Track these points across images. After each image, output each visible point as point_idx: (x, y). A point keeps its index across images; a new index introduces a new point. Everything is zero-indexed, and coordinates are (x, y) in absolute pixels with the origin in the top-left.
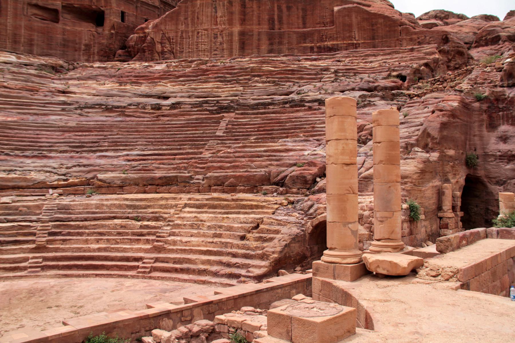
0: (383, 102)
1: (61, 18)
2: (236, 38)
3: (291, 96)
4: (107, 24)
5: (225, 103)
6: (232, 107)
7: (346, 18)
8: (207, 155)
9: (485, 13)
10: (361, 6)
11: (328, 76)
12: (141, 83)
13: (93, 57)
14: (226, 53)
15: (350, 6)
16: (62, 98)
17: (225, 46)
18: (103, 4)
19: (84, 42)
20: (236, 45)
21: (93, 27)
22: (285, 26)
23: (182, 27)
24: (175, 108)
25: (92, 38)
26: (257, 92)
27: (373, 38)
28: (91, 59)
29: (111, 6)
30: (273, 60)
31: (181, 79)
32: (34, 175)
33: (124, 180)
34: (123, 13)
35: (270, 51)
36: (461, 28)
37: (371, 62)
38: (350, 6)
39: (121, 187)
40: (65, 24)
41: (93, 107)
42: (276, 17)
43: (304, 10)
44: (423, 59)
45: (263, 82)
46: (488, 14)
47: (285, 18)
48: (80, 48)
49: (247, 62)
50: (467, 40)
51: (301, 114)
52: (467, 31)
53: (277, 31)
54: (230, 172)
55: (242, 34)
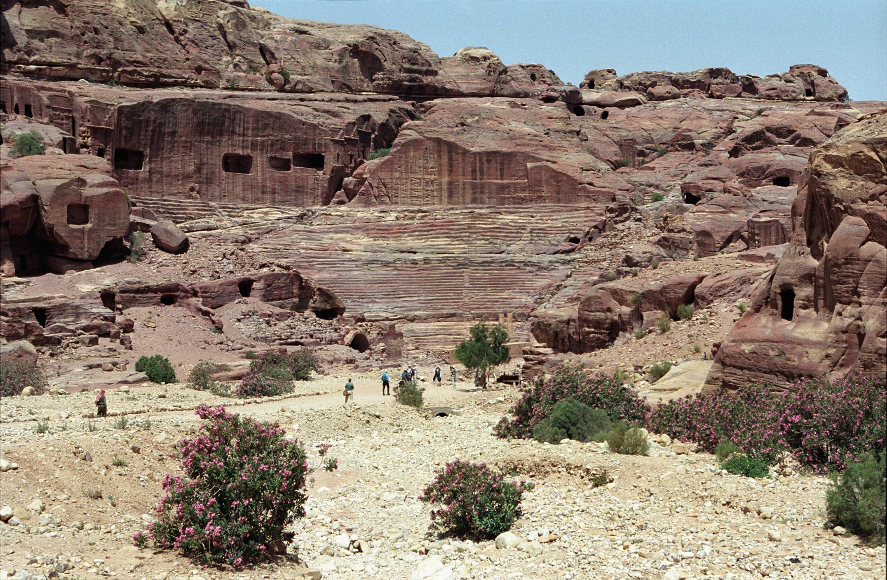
0: (563, 267)
2: (445, 187)
3: (503, 255)
5: (461, 260)
6: (466, 264)
7: (537, 175)
8: (467, 300)
9: (710, 67)
10: (549, 164)
11: (526, 235)
14: (436, 200)
15: (539, 164)
17: (435, 193)
20: (445, 194)
22: (485, 177)
23: (397, 175)
24: (427, 263)
26: (478, 249)
27: (559, 193)
30: (481, 214)
31: (417, 233)
32: (381, 314)
33: (428, 315)
34: (338, 155)
35: (474, 200)
36: (661, 121)
37: (556, 219)
38: (539, 164)
39: (425, 320)
41: (372, 262)
42: (478, 169)
43: (502, 164)
44: (594, 221)
45: (480, 240)
46: (715, 67)
47: (485, 169)
49: (459, 214)
50: (664, 140)
51: (513, 272)
52: (666, 126)
53: (478, 181)
54: (484, 311)
55: (450, 183)
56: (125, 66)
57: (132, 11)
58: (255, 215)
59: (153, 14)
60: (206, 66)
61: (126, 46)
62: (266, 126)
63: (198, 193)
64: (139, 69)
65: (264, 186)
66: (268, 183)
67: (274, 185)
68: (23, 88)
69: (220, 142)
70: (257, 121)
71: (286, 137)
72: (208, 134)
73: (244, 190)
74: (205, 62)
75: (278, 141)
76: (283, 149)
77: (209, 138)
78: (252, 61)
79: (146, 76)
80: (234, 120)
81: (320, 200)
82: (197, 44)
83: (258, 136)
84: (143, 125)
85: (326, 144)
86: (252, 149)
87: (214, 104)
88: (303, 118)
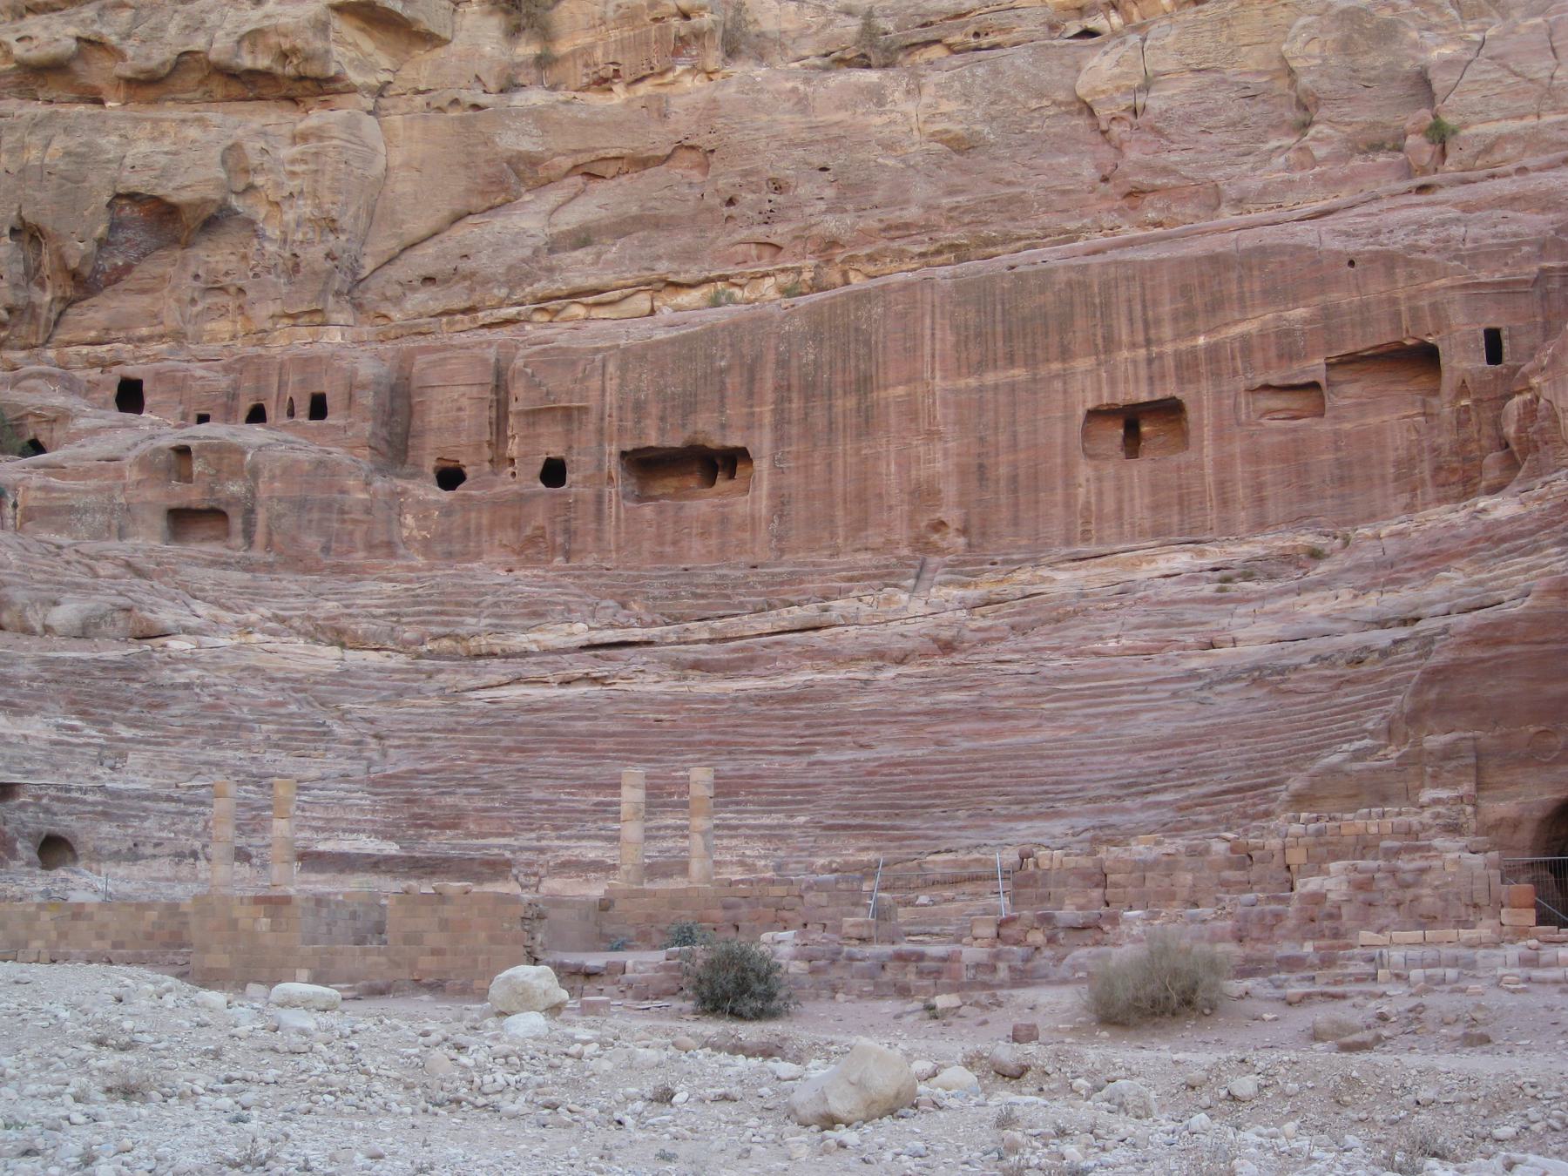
1: (1328, 404)
4: (1448, 381)
12: (1407, 580)
13: (1423, 494)
16: (1196, 662)
18: (1431, 328)
19: (1391, 455)
21: (1413, 404)
25: (1414, 437)
28: (1419, 501)
29: (1449, 326)
40: (1338, 418)
48: (1383, 477)
56: (855, 244)
57: (946, 107)
58: (1062, 576)
59: (1041, 95)
60: (1158, 182)
61: (879, 196)
62: (1216, 306)
63: (964, 531)
64: (895, 245)
65: (1221, 484)
66: (1240, 470)
67: (1257, 474)
68: (306, 360)
69: (1064, 376)
70: (1184, 291)
71: (1300, 312)
72: (1011, 360)
73: (1155, 508)
74: (1166, 171)
75: (1263, 335)
76: (1288, 355)
77: (1019, 373)
78: (1373, 125)
79: (923, 255)
80: (1106, 305)
81: (1431, 491)
82: (1159, 132)
83: (1194, 334)
84: (732, 380)
85: (1434, 307)
86: (1181, 380)
87: (1020, 276)
88: (1354, 246)
